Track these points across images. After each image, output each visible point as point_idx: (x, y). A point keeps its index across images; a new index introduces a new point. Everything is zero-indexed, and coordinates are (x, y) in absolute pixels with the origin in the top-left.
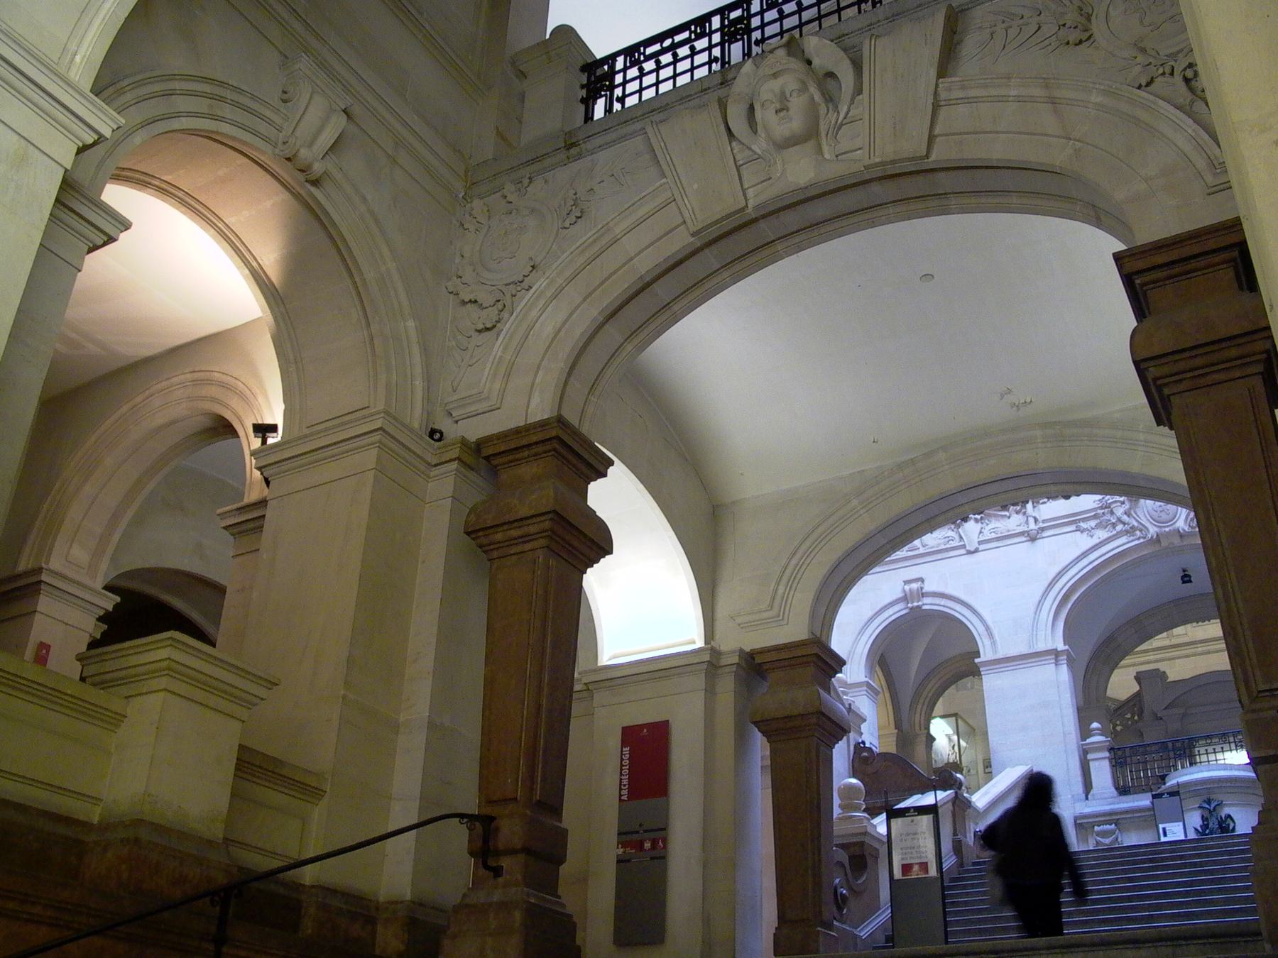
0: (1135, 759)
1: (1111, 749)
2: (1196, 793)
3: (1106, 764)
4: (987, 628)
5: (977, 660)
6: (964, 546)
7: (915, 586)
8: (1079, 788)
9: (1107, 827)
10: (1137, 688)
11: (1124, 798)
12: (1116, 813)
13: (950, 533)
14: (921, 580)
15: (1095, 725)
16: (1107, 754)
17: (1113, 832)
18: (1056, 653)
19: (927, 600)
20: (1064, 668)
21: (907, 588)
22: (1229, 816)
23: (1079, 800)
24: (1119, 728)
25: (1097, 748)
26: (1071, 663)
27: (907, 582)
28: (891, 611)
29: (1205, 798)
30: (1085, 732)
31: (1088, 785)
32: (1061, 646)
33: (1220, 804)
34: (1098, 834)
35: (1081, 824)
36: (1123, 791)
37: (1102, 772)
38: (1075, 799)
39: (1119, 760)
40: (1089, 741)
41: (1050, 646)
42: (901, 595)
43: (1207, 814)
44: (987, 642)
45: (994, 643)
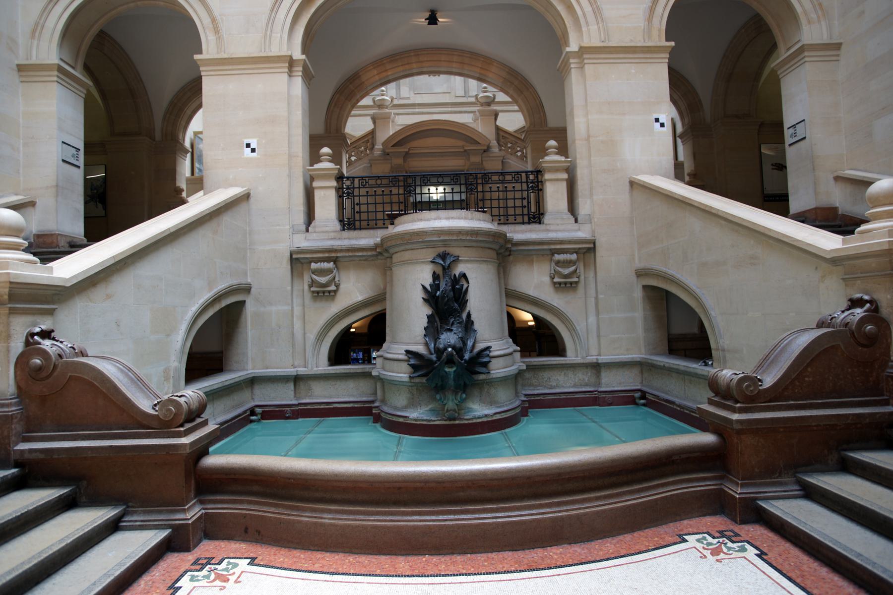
0: (363, 191)
1: (340, 178)
2: (431, 245)
3: (332, 195)
4: (214, 20)
5: (197, 57)
8: (300, 218)
9: (326, 265)
10: (372, 127)
11: (346, 234)
12: (336, 251)
15: (326, 150)
16: (334, 184)
17: (330, 271)
18: (291, 63)
20: (298, 84)
22: (464, 276)
23: (298, 232)
24: (353, 158)
25: (324, 176)
26: (308, 77)
29: (441, 250)
30: (314, 157)
32: (298, 55)
33: (457, 260)
34: (314, 272)
35: (297, 259)
36: (348, 223)
37: (327, 204)
38: (295, 231)
39: (345, 189)
40: (316, 166)
41: (285, 52)
43: (439, 271)
44: (212, 37)
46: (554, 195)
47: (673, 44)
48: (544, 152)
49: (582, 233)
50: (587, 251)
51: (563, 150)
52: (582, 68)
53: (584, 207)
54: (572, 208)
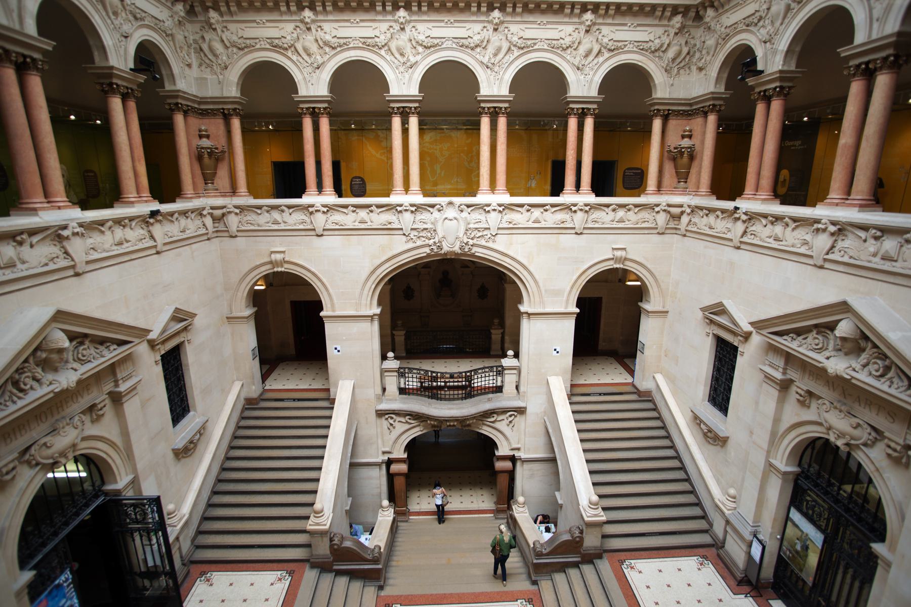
0: (410, 375)
5: (322, 314)
6: (314, 230)
7: (279, 257)
8: (380, 391)
13: (304, 217)
14: (283, 252)
18: (372, 317)
19: (286, 266)
21: (273, 256)
27: (272, 252)
28: (263, 269)
30: (384, 357)
31: (384, 390)
37: (392, 384)
41: (370, 313)
42: (267, 260)
45: (333, 305)
46: (510, 379)
47: (578, 310)
48: (505, 356)
49: (520, 404)
50: (521, 411)
51: (517, 356)
52: (529, 318)
53: (522, 389)
54: (517, 388)
